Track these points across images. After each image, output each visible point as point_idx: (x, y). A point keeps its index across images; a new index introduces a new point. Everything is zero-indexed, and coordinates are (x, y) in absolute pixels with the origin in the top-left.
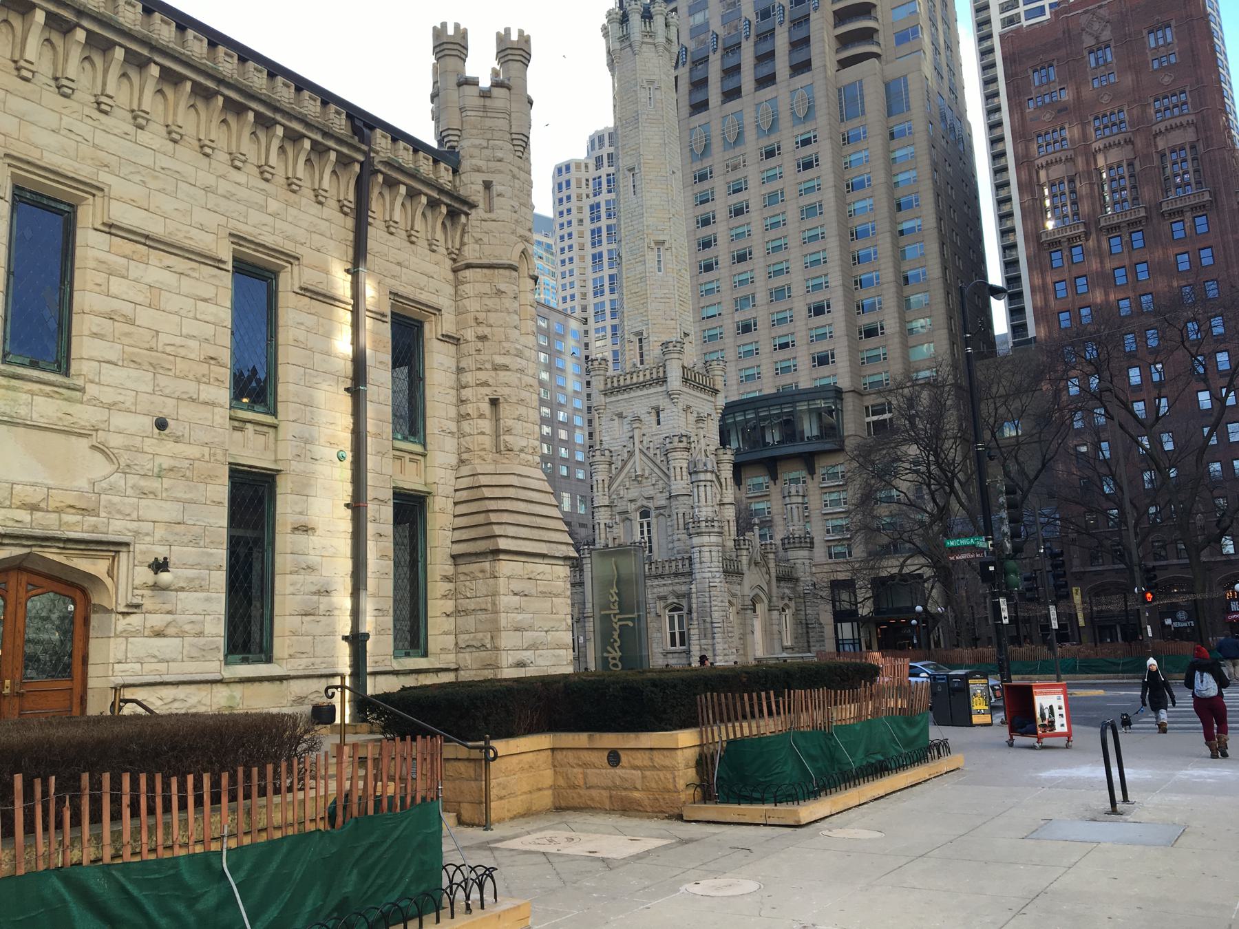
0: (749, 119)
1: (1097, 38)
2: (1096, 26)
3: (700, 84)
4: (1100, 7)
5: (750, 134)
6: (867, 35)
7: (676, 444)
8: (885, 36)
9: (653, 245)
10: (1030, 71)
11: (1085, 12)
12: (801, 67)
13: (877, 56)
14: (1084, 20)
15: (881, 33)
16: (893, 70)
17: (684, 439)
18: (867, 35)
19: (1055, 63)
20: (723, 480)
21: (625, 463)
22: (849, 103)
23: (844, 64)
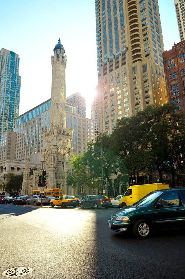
0: (114, 76)
1: (182, 52)
2: (181, 49)
3: (105, 69)
4: (182, 45)
5: (114, 79)
6: (139, 56)
7: (54, 147)
8: (143, 56)
9: (56, 104)
10: (168, 60)
11: (179, 46)
12: (124, 64)
13: (141, 60)
14: (179, 48)
15: (142, 55)
16: (144, 63)
17: (56, 146)
18: (139, 56)
19: (173, 58)
20: (71, 155)
21: (47, 151)
22: (134, 70)
23: (134, 62)
